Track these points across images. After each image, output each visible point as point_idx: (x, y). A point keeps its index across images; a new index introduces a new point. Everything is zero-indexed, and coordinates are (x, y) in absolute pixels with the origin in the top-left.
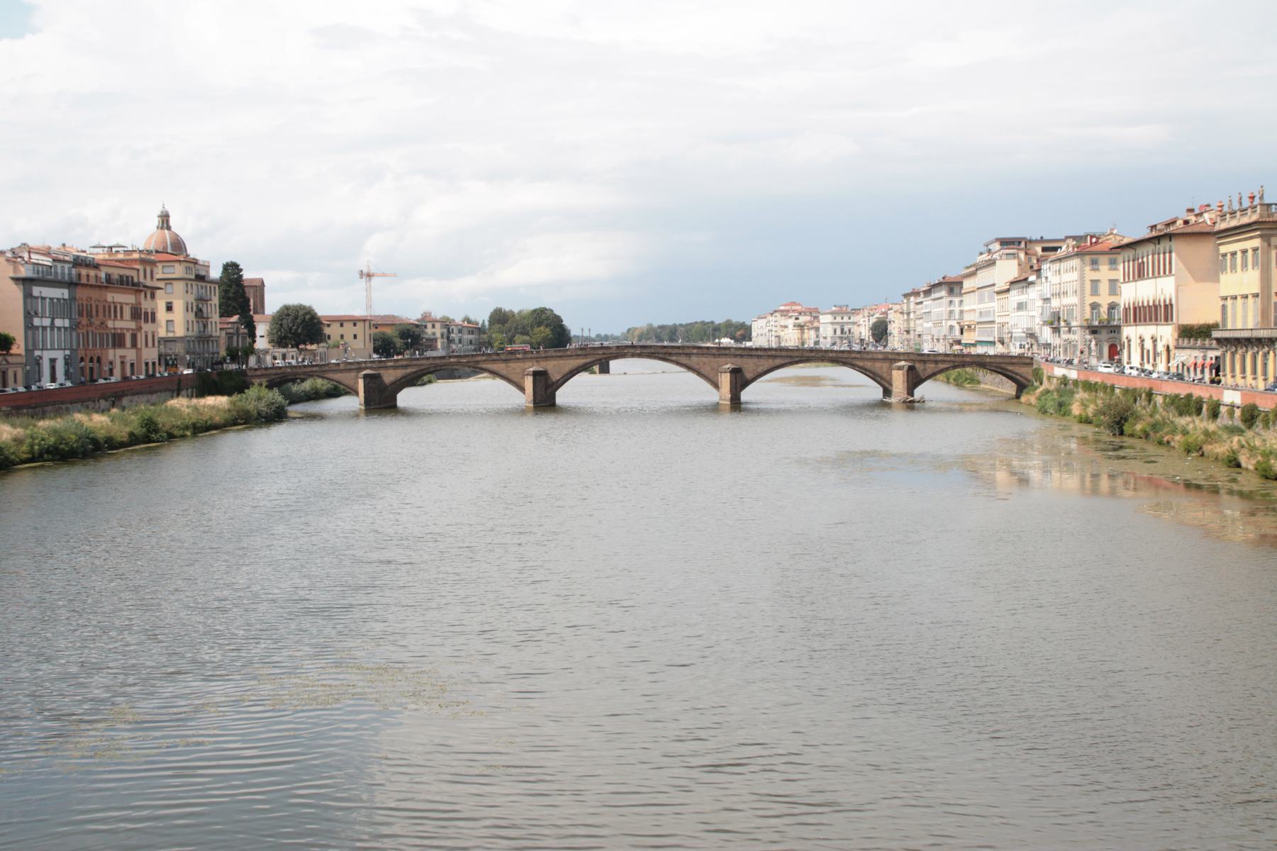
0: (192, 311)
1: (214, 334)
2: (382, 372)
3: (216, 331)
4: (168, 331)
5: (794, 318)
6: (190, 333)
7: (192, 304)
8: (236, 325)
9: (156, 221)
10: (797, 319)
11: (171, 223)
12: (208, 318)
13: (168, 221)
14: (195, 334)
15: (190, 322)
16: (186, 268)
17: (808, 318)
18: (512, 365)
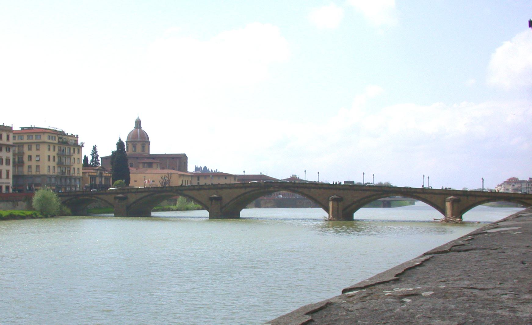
0: (54, 160)
1: (76, 175)
2: (129, 195)
3: (79, 173)
4: (36, 171)
5: (512, 185)
6: (51, 173)
7: (54, 157)
8: (98, 172)
9: (134, 125)
10: (514, 186)
11: (142, 126)
12: (71, 166)
13: (140, 124)
14: (56, 174)
15: (51, 168)
16: (49, 136)
17: (520, 185)
18: (201, 192)
